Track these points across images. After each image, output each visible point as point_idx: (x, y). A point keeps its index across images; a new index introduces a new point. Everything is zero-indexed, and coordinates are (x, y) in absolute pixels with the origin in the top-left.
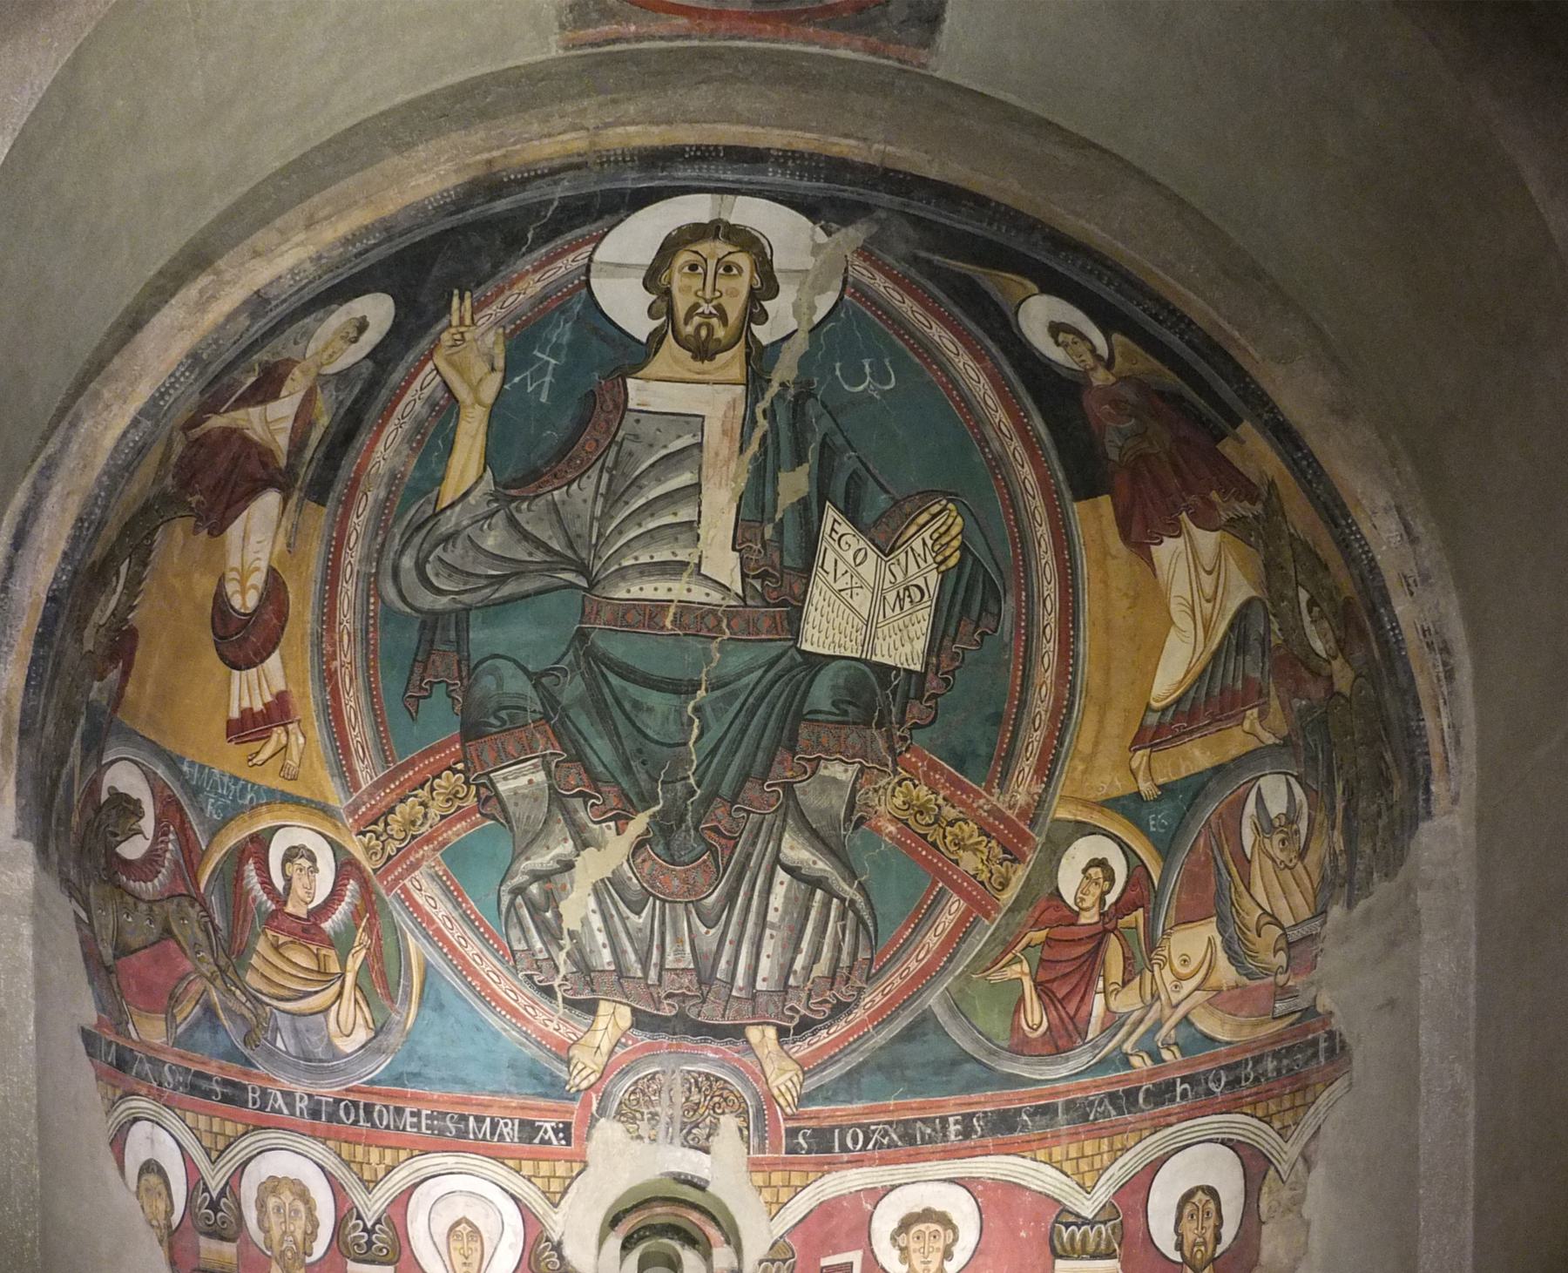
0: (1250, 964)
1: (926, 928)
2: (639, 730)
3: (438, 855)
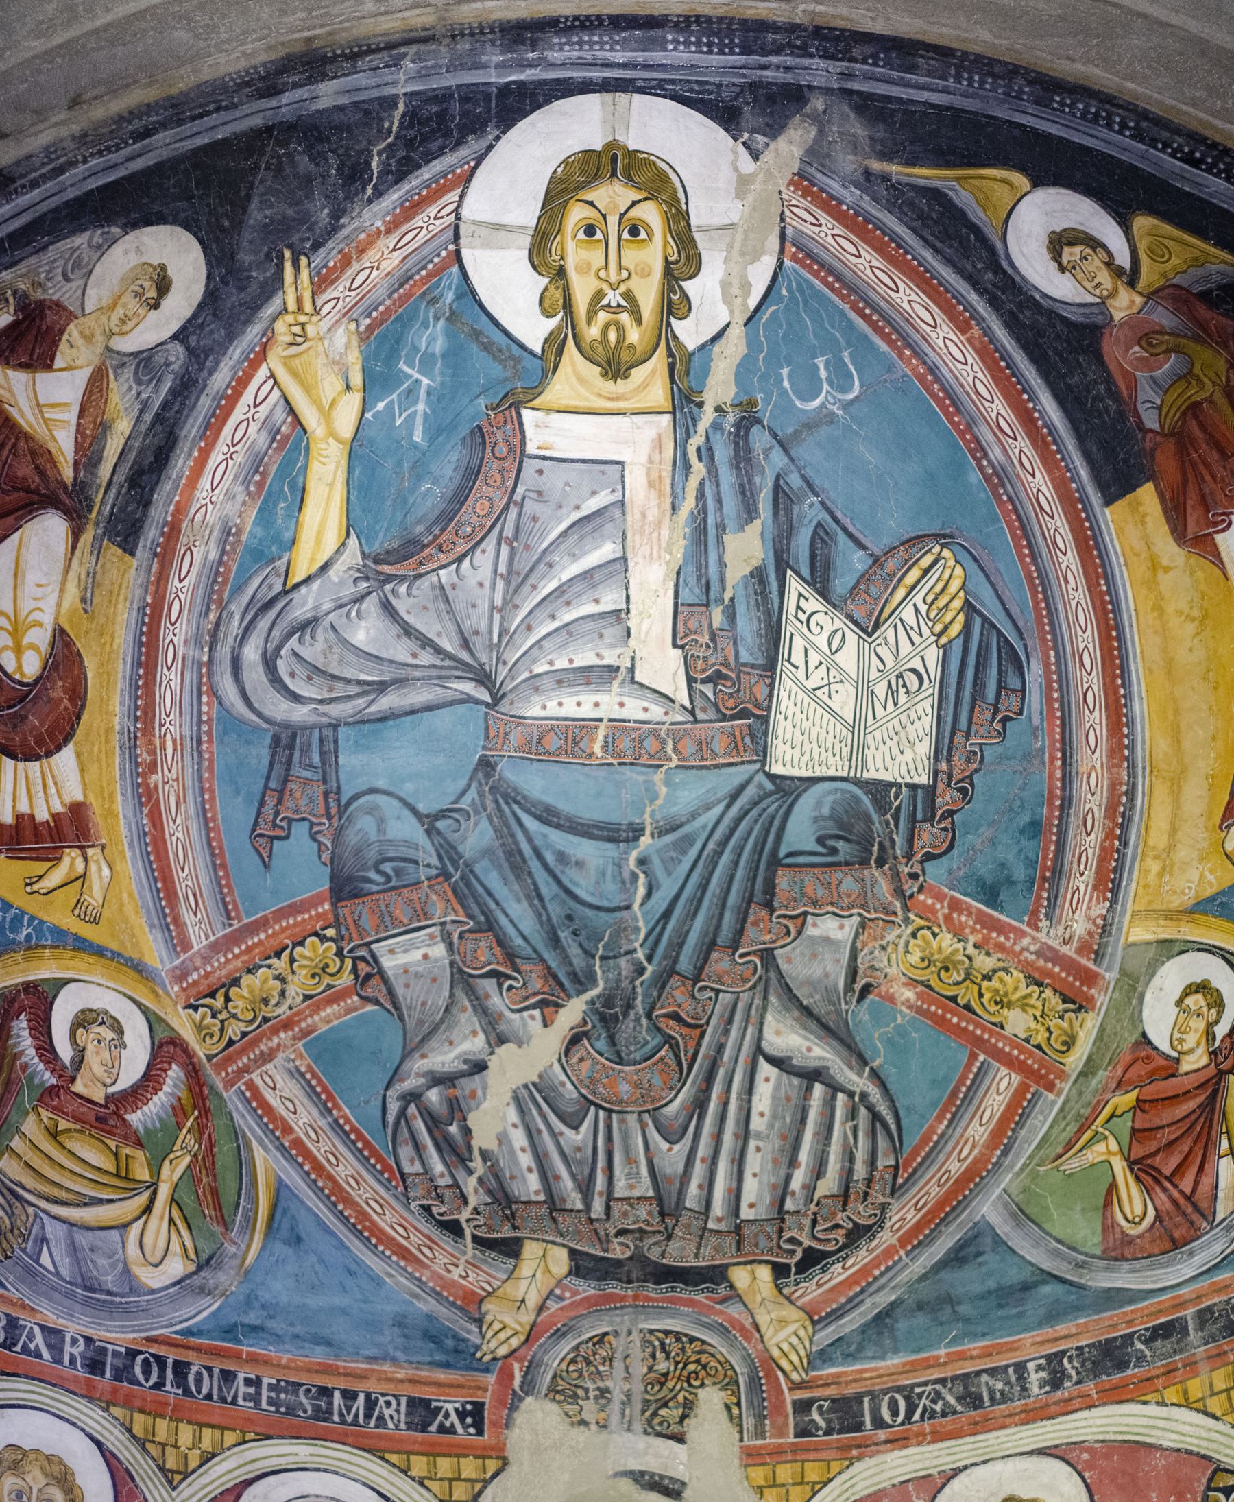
1: (968, 1116)
2: (569, 892)
3: (300, 1045)
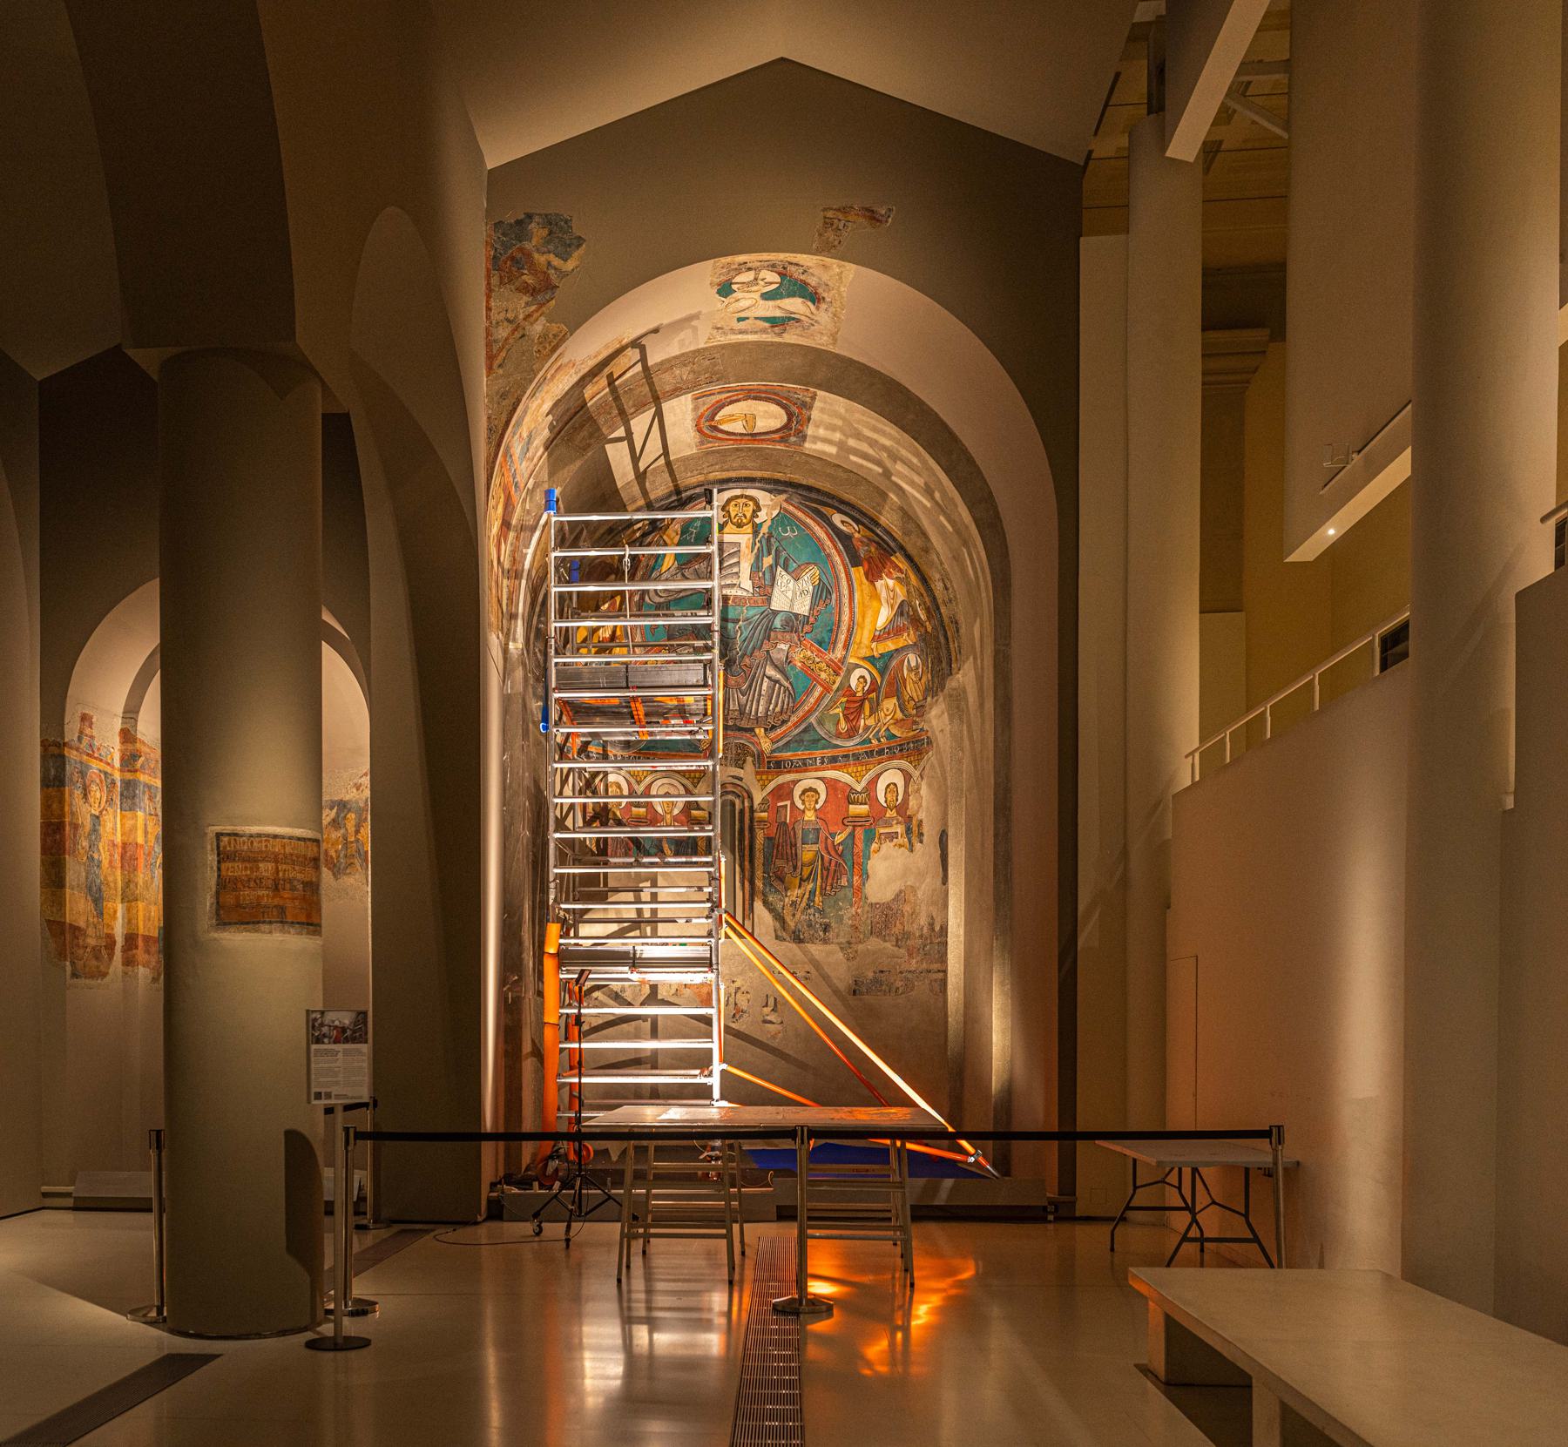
0: (906, 712)
